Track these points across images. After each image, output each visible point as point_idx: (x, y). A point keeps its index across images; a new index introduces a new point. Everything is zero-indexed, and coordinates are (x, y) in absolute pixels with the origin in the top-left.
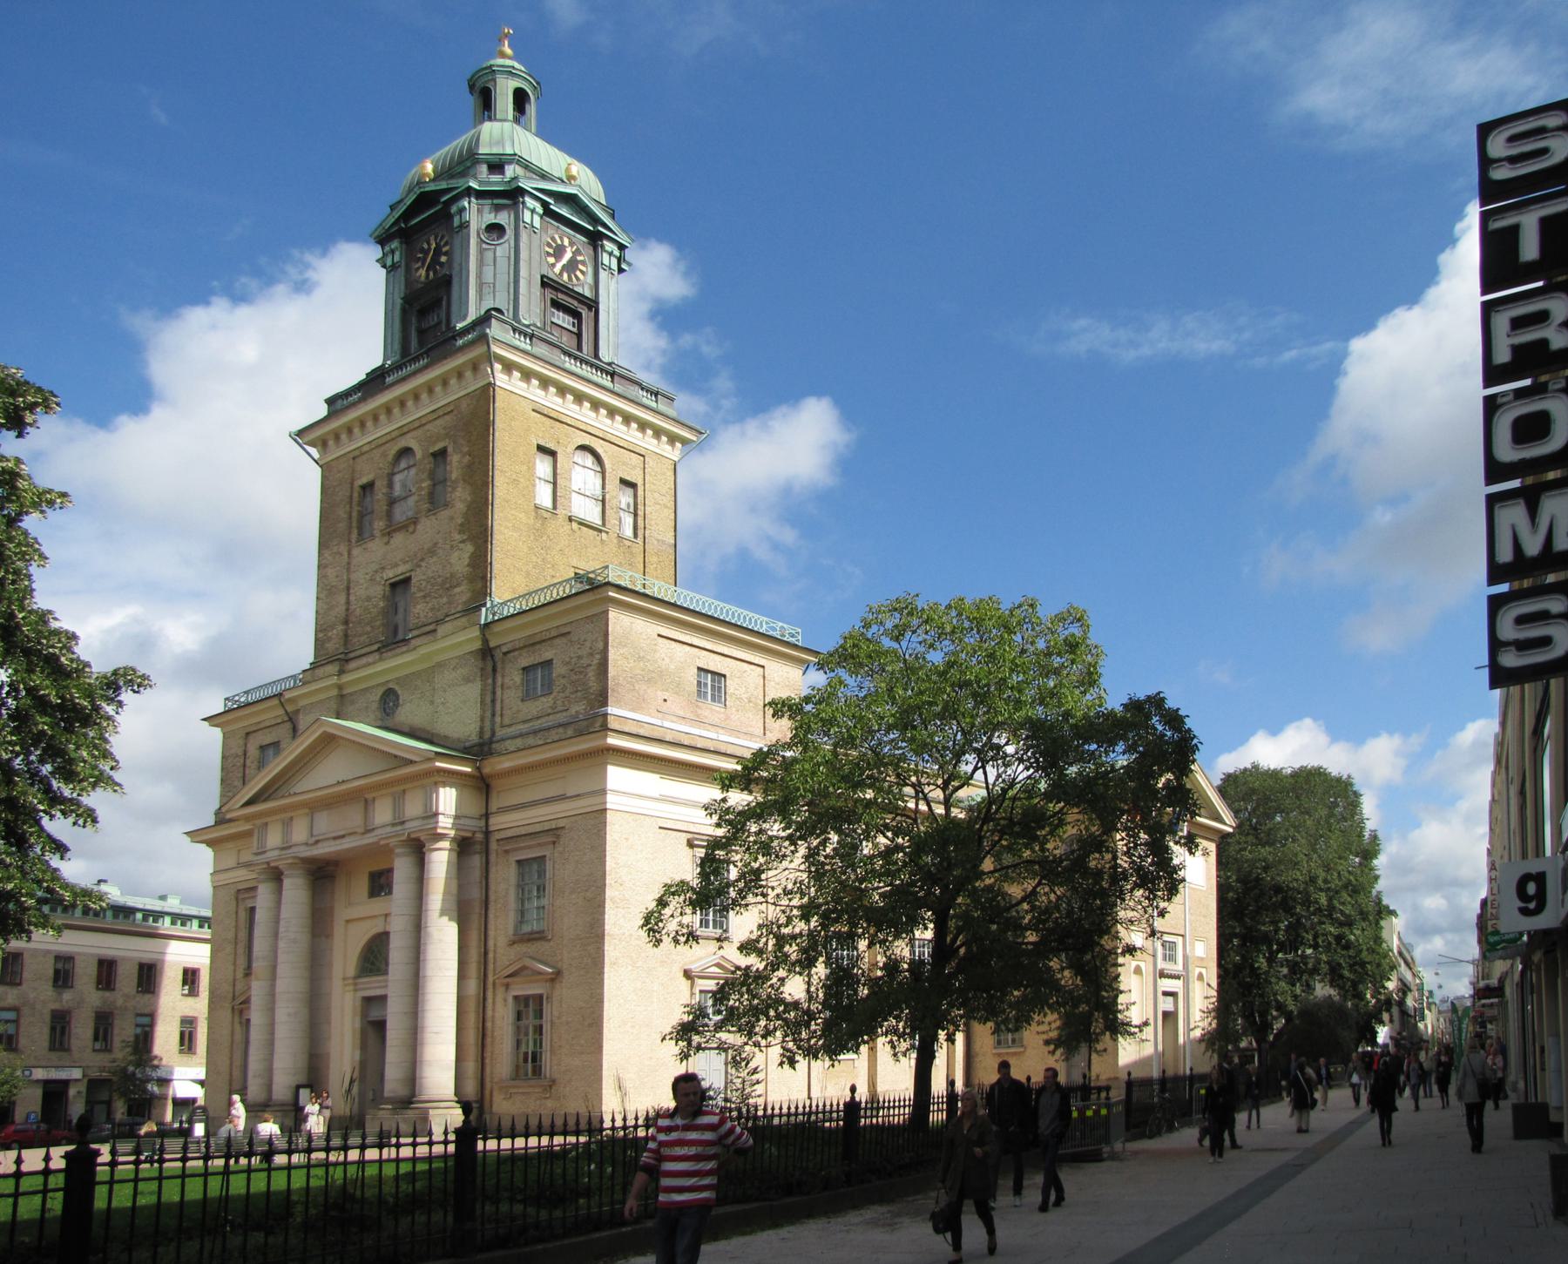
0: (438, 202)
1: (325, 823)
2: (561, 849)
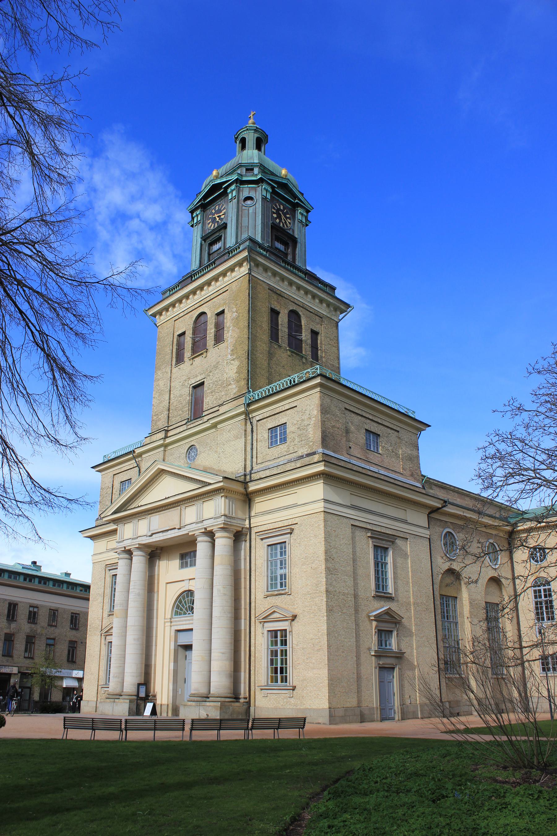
0: (221, 188)
2: (295, 538)
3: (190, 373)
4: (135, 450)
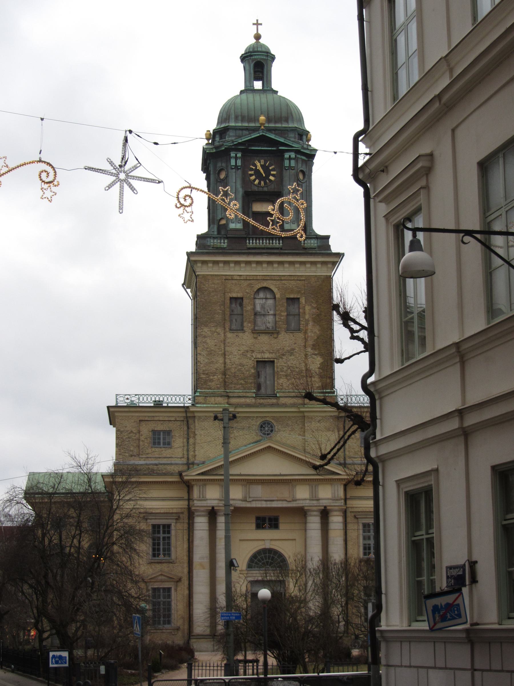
1: (258, 491)
3: (254, 345)
4: (190, 408)
